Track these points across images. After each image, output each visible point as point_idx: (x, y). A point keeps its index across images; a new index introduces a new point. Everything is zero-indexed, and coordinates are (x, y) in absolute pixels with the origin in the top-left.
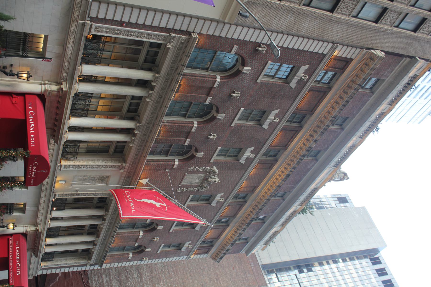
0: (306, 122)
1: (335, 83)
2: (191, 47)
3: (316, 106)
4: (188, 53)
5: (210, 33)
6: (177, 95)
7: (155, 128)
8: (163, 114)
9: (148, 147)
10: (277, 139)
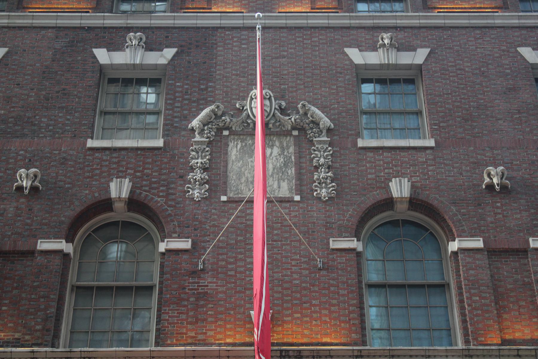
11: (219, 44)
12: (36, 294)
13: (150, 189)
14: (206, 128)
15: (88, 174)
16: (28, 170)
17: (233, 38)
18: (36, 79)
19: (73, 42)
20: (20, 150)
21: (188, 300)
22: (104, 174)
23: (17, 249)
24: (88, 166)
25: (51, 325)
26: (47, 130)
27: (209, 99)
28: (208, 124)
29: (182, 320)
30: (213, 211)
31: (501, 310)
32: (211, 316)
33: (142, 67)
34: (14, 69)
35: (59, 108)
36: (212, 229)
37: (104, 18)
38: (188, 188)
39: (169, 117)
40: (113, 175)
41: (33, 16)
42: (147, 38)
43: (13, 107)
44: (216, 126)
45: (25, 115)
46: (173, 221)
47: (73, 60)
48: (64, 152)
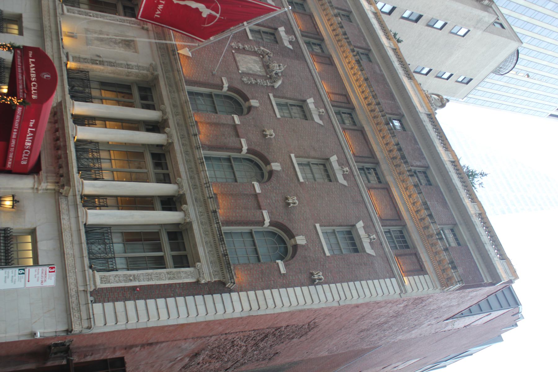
31: (211, 124)
37: (378, 222)
42: (294, 42)
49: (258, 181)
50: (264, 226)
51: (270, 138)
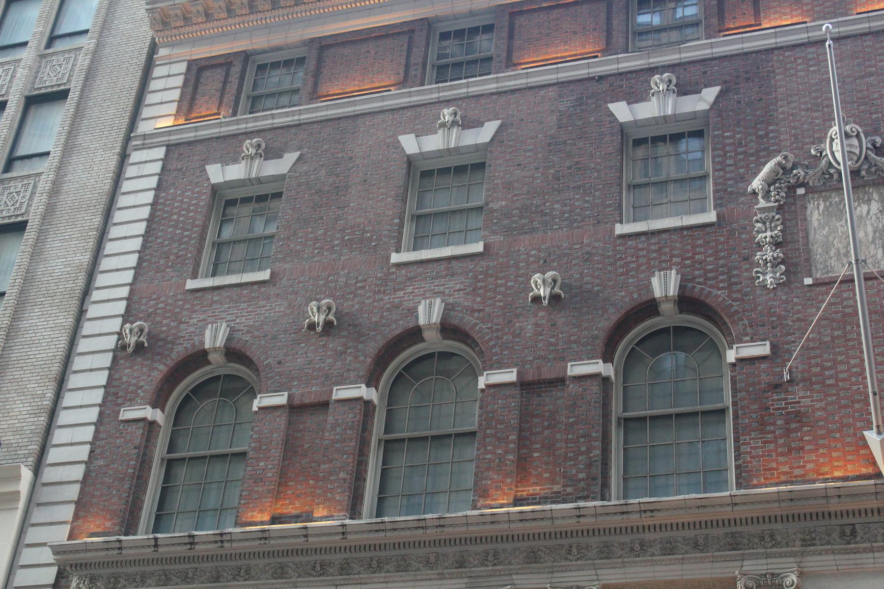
0: (472, 14)
1: (288, 47)
2: (87, 551)
3: (387, 36)
4: (107, 549)
5: (68, 512)
6: (319, 512)
7: (464, 529)
8: (382, 527)
9: (582, 520)
10: (566, 50)
11: (778, 71)
12: (573, 433)
13: (705, 280)
14: (772, 188)
15: (621, 270)
16: (544, 274)
17: (795, 59)
18: (540, 155)
19: (581, 98)
20: (531, 250)
21: (774, 424)
22: (642, 268)
23: (542, 377)
24: (620, 259)
25: (597, 471)
26: (562, 219)
27: (772, 148)
28: (774, 183)
29: (769, 451)
30: (795, 300)
32: (809, 442)
33: (675, 118)
34: (511, 146)
35: (574, 188)
36: (797, 325)
38: (757, 272)
39: (721, 180)
40: (654, 267)
41: (527, 73)
42: (678, 78)
43: (515, 195)
44: (786, 184)
45: (532, 204)
46: (741, 319)
47: (583, 123)
48: (588, 245)
49: (252, 394)
50: (376, 401)
51: (149, 334)
